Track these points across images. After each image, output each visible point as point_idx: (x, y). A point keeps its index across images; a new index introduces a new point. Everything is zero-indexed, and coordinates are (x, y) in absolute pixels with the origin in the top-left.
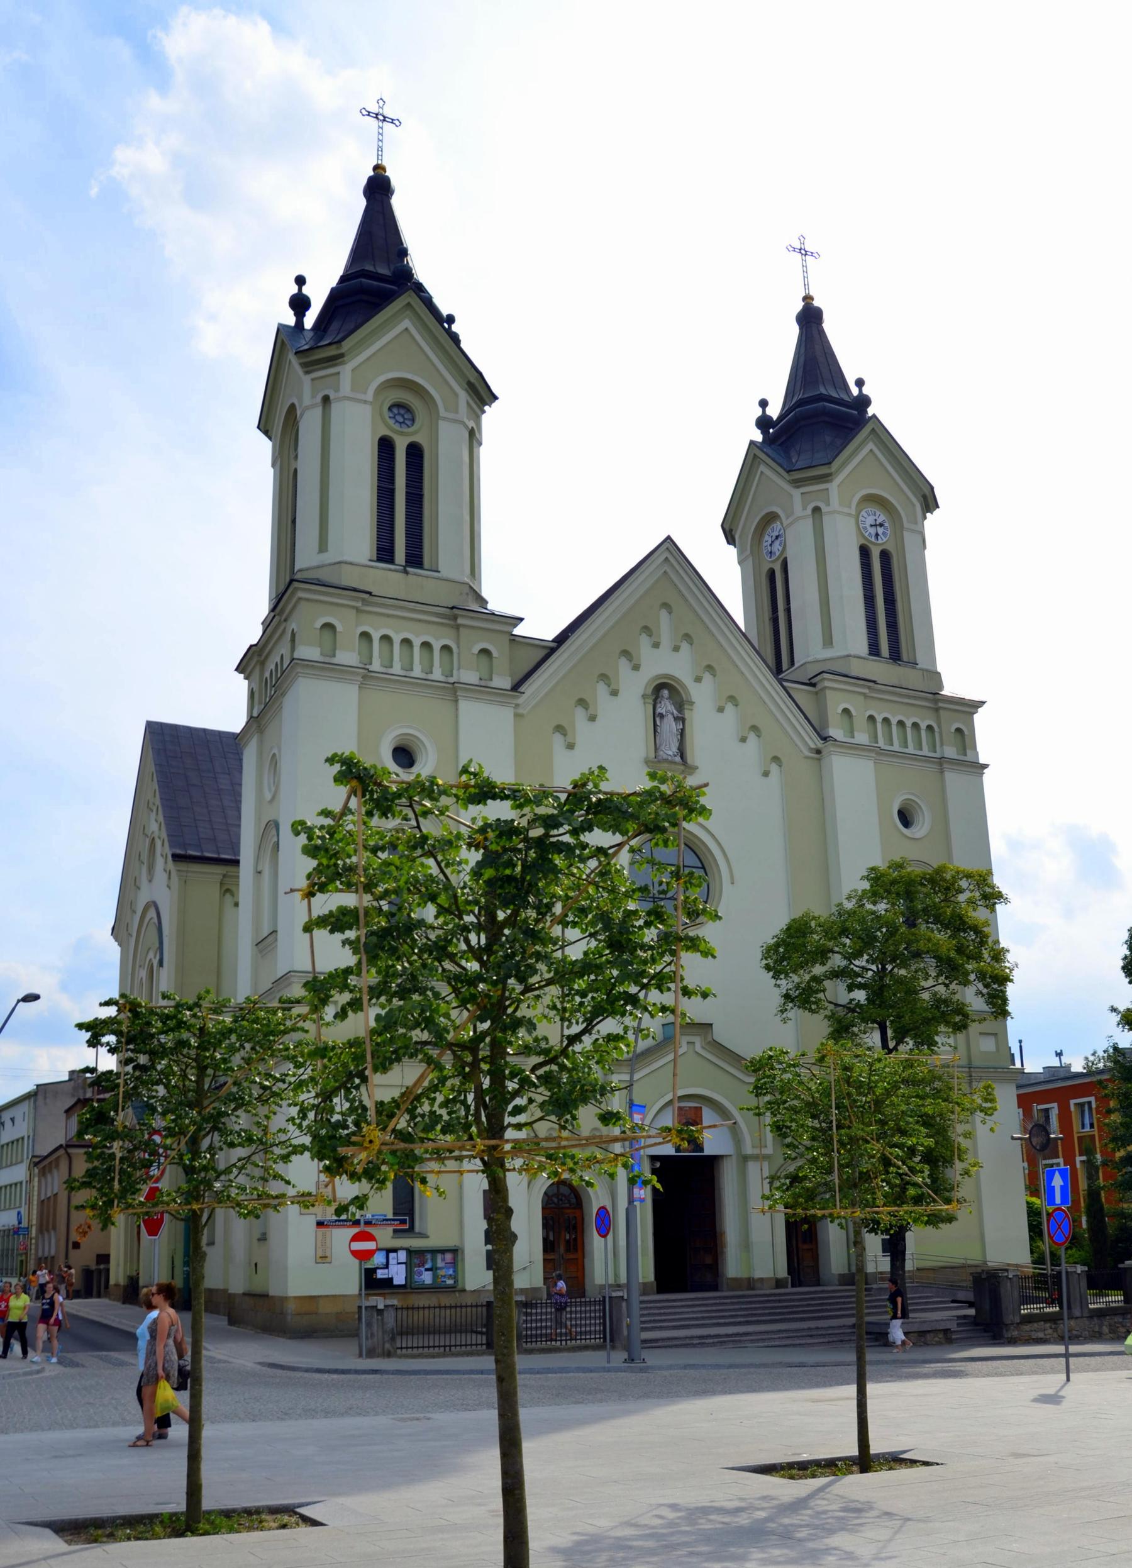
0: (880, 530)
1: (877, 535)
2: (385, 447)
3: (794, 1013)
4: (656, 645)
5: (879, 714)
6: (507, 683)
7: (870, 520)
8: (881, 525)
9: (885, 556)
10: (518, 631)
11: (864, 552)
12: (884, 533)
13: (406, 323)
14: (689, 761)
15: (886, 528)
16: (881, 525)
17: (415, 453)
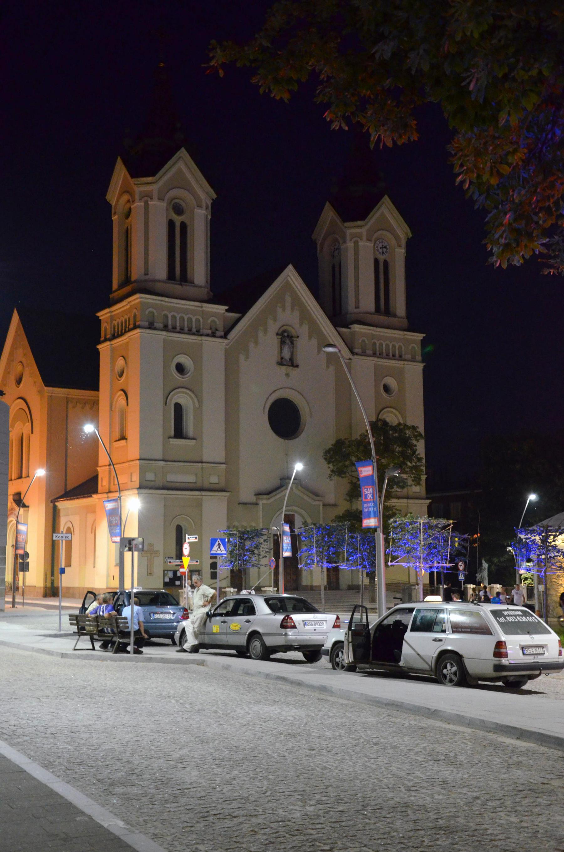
0: (385, 250)
1: (383, 253)
2: (171, 224)
3: (335, 478)
4: (284, 310)
5: (378, 341)
6: (222, 334)
7: (380, 245)
8: (385, 247)
9: (386, 263)
10: (227, 308)
11: (376, 261)
12: (386, 252)
13: (181, 165)
14: (295, 364)
15: (387, 249)
16: (385, 247)
17: (184, 226)
